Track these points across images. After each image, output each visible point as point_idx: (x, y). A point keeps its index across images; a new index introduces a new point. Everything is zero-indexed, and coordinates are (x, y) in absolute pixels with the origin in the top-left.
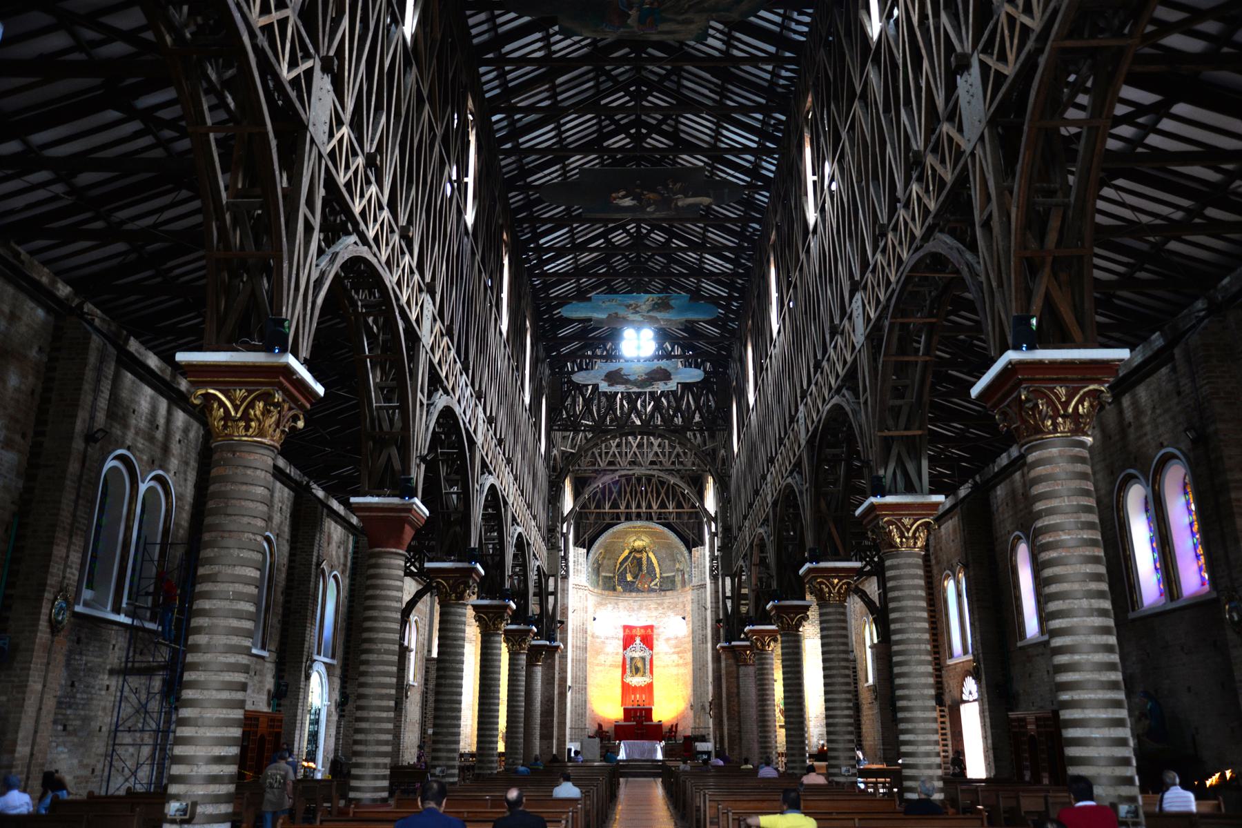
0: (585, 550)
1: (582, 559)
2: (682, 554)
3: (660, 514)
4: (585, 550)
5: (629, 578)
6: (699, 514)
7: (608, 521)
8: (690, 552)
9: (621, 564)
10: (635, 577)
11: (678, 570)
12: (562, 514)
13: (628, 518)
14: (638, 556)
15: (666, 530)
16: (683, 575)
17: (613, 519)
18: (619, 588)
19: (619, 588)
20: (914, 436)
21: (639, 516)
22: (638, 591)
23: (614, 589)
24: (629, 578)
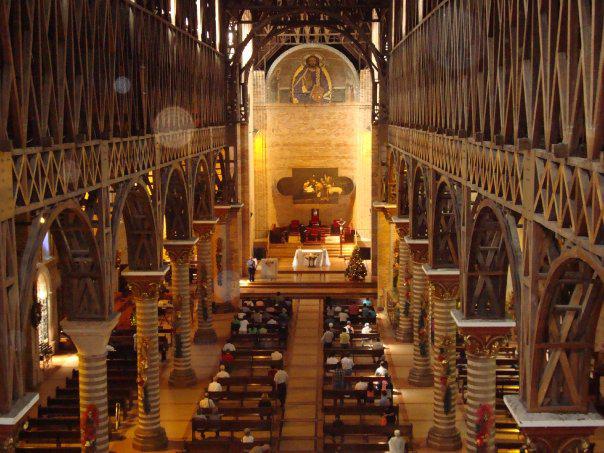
0: (263, 73)
1: (261, 82)
2: (351, 72)
3: (332, 37)
4: (263, 73)
5: (304, 90)
6: (368, 48)
7: (283, 43)
8: (359, 72)
9: (297, 78)
10: (310, 89)
11: (348, 85)
12: (240, 64)
13: (303, 40)
14: (312, 70)
15: (337, 52)
16: (352, 90)
17: (288, 41)
18: (295, 100)
19: (295, 100)
20: (509, 328)
21: (312, 38)
22: (313, 102)
23: (291, 102)
24: (304, 90)
